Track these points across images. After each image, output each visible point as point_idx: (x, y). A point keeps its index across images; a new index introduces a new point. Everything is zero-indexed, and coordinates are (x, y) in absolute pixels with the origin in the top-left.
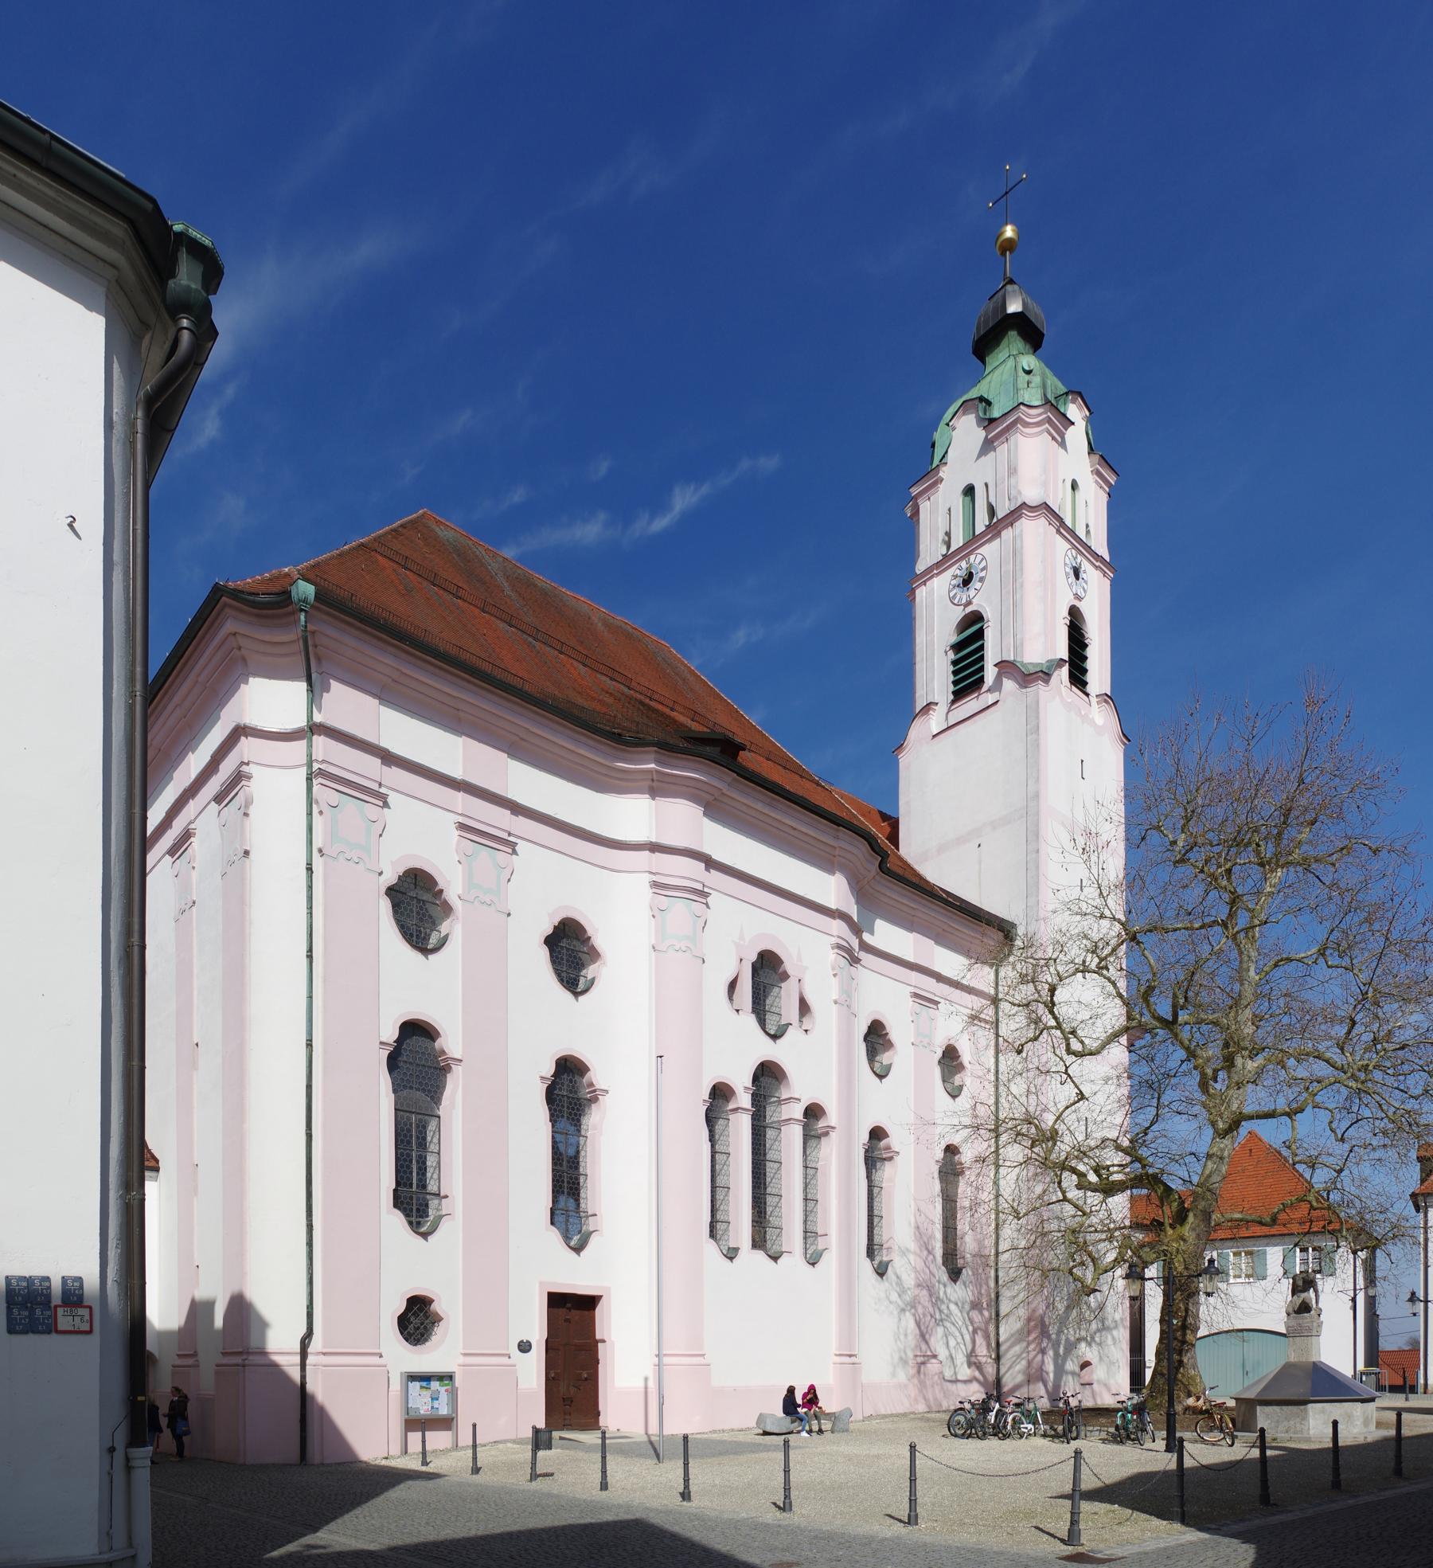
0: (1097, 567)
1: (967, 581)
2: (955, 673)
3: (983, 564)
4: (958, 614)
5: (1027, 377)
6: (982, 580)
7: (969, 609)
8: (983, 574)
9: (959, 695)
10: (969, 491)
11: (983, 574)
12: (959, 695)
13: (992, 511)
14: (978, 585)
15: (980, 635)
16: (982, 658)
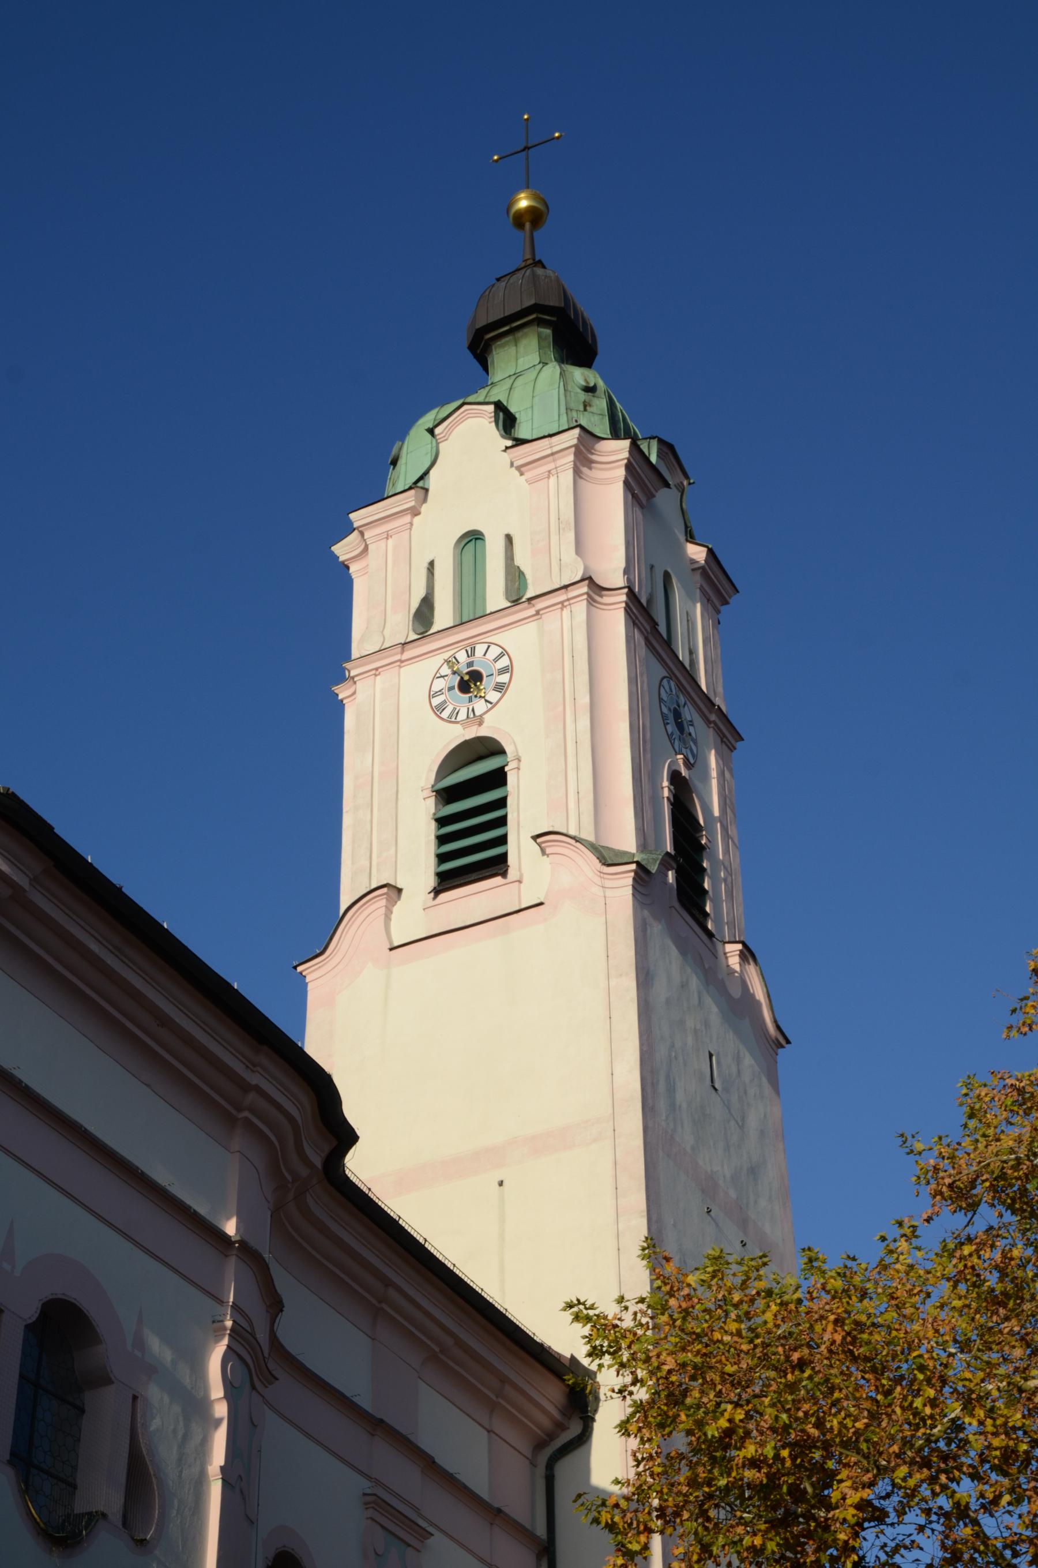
0: (708, 722)
1: (469, 682)
2: (442, 840)
3: (504, 662)
4: (457, 735)
5: (583, 396)
6: (500, 688)
7: (471, 733)
8: (504, 678)
9: (447, 880)
10: (473, 538)
11: (504, 678)
12: (447, 880)
13: (515, 577)
14: (493, 696)
15: (498, 778)
16: (502, 821)
